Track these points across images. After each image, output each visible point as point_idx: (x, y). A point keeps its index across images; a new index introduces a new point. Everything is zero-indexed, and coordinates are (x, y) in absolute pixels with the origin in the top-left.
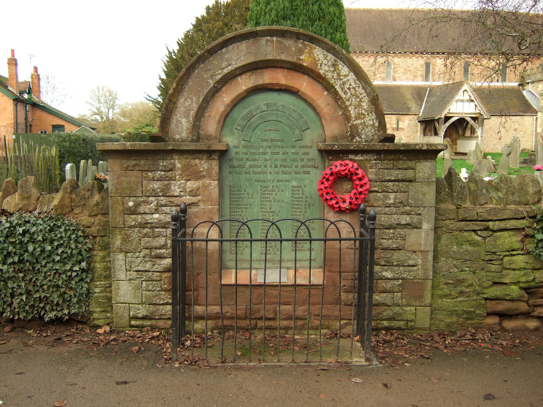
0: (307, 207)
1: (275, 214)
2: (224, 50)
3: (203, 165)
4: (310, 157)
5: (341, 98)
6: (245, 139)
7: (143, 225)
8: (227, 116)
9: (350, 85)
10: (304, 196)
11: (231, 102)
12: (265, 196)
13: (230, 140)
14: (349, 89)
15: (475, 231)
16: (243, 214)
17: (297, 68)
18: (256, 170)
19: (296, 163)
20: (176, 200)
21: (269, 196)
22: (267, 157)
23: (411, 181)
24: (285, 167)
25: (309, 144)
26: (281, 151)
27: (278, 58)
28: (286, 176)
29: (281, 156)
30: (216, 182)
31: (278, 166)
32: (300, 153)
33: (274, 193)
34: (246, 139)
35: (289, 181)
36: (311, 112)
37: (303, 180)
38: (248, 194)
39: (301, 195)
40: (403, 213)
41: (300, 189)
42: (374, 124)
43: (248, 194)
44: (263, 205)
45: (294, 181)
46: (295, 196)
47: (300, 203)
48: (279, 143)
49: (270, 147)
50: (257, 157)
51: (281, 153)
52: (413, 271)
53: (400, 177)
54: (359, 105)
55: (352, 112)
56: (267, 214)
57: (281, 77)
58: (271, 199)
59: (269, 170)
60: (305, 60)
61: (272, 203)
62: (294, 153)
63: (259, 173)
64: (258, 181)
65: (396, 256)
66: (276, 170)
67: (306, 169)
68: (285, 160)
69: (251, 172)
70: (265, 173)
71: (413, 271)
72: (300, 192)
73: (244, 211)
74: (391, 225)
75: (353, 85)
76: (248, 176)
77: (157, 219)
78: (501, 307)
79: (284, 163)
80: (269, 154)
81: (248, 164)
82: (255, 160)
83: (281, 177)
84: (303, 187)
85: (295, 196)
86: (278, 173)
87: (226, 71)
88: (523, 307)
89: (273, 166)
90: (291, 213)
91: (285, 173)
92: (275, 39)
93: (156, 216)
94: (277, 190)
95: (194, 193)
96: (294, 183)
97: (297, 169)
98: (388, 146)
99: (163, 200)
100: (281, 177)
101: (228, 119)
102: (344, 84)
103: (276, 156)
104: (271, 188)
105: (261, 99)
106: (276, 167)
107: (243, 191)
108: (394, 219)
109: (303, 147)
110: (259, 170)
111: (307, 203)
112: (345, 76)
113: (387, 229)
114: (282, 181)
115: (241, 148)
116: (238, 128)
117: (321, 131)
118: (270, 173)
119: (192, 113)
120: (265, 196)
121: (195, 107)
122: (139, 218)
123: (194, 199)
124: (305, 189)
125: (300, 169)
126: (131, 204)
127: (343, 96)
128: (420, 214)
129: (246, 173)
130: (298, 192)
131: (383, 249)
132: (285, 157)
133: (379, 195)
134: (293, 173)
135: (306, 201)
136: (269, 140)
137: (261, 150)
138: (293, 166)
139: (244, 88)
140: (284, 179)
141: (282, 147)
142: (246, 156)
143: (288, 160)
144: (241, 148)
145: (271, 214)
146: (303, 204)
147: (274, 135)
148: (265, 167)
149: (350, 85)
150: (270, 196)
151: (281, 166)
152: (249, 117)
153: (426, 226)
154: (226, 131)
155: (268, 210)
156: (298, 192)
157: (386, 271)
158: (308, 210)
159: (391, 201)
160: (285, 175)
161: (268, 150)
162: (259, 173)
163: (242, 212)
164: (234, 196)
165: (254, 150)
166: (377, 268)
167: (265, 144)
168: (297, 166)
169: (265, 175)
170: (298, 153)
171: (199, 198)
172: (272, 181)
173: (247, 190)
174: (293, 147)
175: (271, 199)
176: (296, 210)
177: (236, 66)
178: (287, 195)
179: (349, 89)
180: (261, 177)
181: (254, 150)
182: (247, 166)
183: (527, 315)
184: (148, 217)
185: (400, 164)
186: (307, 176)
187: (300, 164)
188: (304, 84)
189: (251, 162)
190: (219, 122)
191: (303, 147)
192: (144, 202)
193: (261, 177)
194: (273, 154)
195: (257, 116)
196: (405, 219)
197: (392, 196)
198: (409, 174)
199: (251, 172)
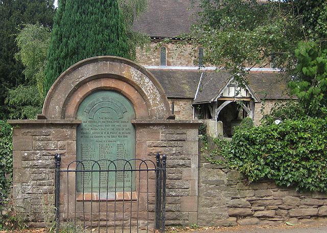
2: (80, 68)
3: (68, 132)
4: (127, 128)
5: (145, 94)
7: (32, 167)
8: (80, 105)
9: (150, 88)
11: (83, 97)
13: (82, 118)
14: (149, 90)
15: (221, 169)
17: (120, 78)
18: (96, 135)
20: (52, 152)
23: (184, 141)
27: (110, 73)
30: (75, 142)
36: (128, 103)
40: (181, 159)
42: (163, 109)
52: (186, 191)
53: (178, 138)
54: (154, 99)
55: (151, 103)
57: (112, 83)
59: (104, 135)
60: (125, 74)
62: (118, 126)
65: (177, 183)
67: (125, 135)
68: (113, 129)
71: (186, 191)
74: (174, 165)
75: (151, 87)
77: (41, 163)
78: (237, 211)
79: (112, 131)
81: (92, 131)
82: (96, 129)
83: (111, 139)
87: (81, 80)
88: (249, 211)
91: (114, 137)
92: (108, 62)
93: (40, 161)
95: (62, 148)
96: (119, 143)
98: (172, 121)
99: (45, 152)
100: (111, 139)
101: (81, 106)
102: (147, 87)
105: (100, 96)
108: (176, 162)
109: (123, 122)
112: (147, 83)
113: (172, 167)
114: (111, 142)
117: (133, 113)
118: (105, 137)
119: (62, 103)
121: (64, 100)
122: (31, 163)
123: (62, 152)
126: (26, 154)
127: (146, 94)
128: (190, 159)
131: (169, 179)
132: (113, 127)
133: (167, 148)
137: (99, 124)
139: (90, 89)
143: (115, 129)
147: (106, 115)
149: (150, 88)
152: (93, 105)
153: (193, 166)
154: (80, 113)
157: (172, 191)
159: (174, 152)
166: (167, 190)
167: (101, 120)
168: (119, 133)
170: (120, 126)
171: (65, 151)
177: (86, 77)
178: (114, 149)
179: (149, 90)
180: (100, 139)
182: (91, 133)
183: (251, 215)
184: (35, 162)
185: (179, 131)
186: (126, 138)
187: (121, 131)
188: (124, 87)
190: (76, 108)
191: (123, 122)
192: (33, 153)
193: (100, 139)
196: (181, 162)
197: (174, 149)
198: (183, 137)
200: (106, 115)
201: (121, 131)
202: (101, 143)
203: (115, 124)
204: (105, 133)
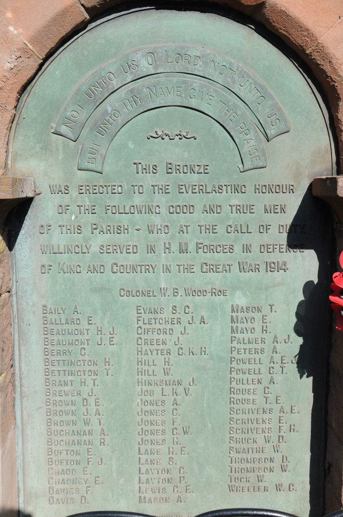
0: (277, 367)
1: (180, 390)
6: (86, 165)
10: (269, 338)
11: (34, 40)
12: (149, 336)
16: (85, 390)
19: (245, 239)
21: (162, 337)
22: (157, 220)
24: (211, 249)
25: (285, 180)
26: (199, 201)
28: (216, 279)
29: (199, 217)
31: (192, 247)
32: (259, 208)
33: (178, 328)
34: (91, 166)
35: (221, 292)
37: (267, 288)
38: (100, 331)
39: (258, 333)
41: (258, 316)
43: (100, 331)
44: (147, 363)
45: (238, 293)
46: (240, 336)
47: (257, 357)
48: (194, 178)
49: (165, 190)
50: (124, 220)
51: (199, 208)
56: (158, 389)
58: (170, 345)
59: (163, 258)
61: (173, 358)
62: (239, 209)
63: (134, 269)
64: (129, 293)
66: (185, 259)
68: (212, 229)
69: (108, 267)
70: (149, 268)
72: (258, 325)
73: (90, 382)
76: (97, 277)
79: (207, 239)
80: (163, 210)
82: (119, 230)
83: (198, 280)
84: (266, 310)
85: (240, 336)
86: (189, 269)
89: (175, 247)
90: (228, 386)
91: (214, 268)
94: (185, 319)
96: (241, 300)
97: (249, 258)
100: (198, 280)
103: (182, 219)
104: (167, 314)
106: (183, 250)
107: (84, 324)
109: (270, 189)
110: (133, 259)
111: (277, 358)
114: (203, 292)
115: (74, 192)
116: (64, 129)
118: (167, 269)
120: (149, 336)
124: (271, 317)
125: (255, 256)
129: (93, 270)
130: (249, 325)
132: (210, 218)
134: (235, 268)
135: (275, 351)
136: (161, 169)
137: (138, 200)
138: (238, 248)
140: (209, 288)
141: (202, 190)
142: (92, 218)
143: (221, 230)
144: (74, 192)
145: (168, 390)
146: (265, 358)
147: (177, 153)
148: (151, 249)
150: (167, 337)
151: (198, 246)
152: (96, 95)
155: (160, 376)
156: (249, 325)
158: (278, 378)
160: (211, 275)
161: (161, 199)
162: (134, 269)
163: (83, 383)
164: (56, 338)
165: (115, 200)
167: (149, 180)
168: (247, 249)
169: (151, 275)
170: (250, 208)
172: (170, 292)
173: (97, 320)
174: (237, 189)
175: (170, 345)
176: (245, 377)
178: (217, 334)
180: (140, 280)
181: (115, 200)
182: (95, 249)
186: (278, 276)
187: (256, 240)
189: (107, 236)
191: (270, 189)
193: (140, 280)
194: (174, 209)
195: (122, 93)
199: (108, 267)
200: (177, 153)
201: (256, 240)
202: (150, 302)
203: (217, 198)
204: (168, 248)
